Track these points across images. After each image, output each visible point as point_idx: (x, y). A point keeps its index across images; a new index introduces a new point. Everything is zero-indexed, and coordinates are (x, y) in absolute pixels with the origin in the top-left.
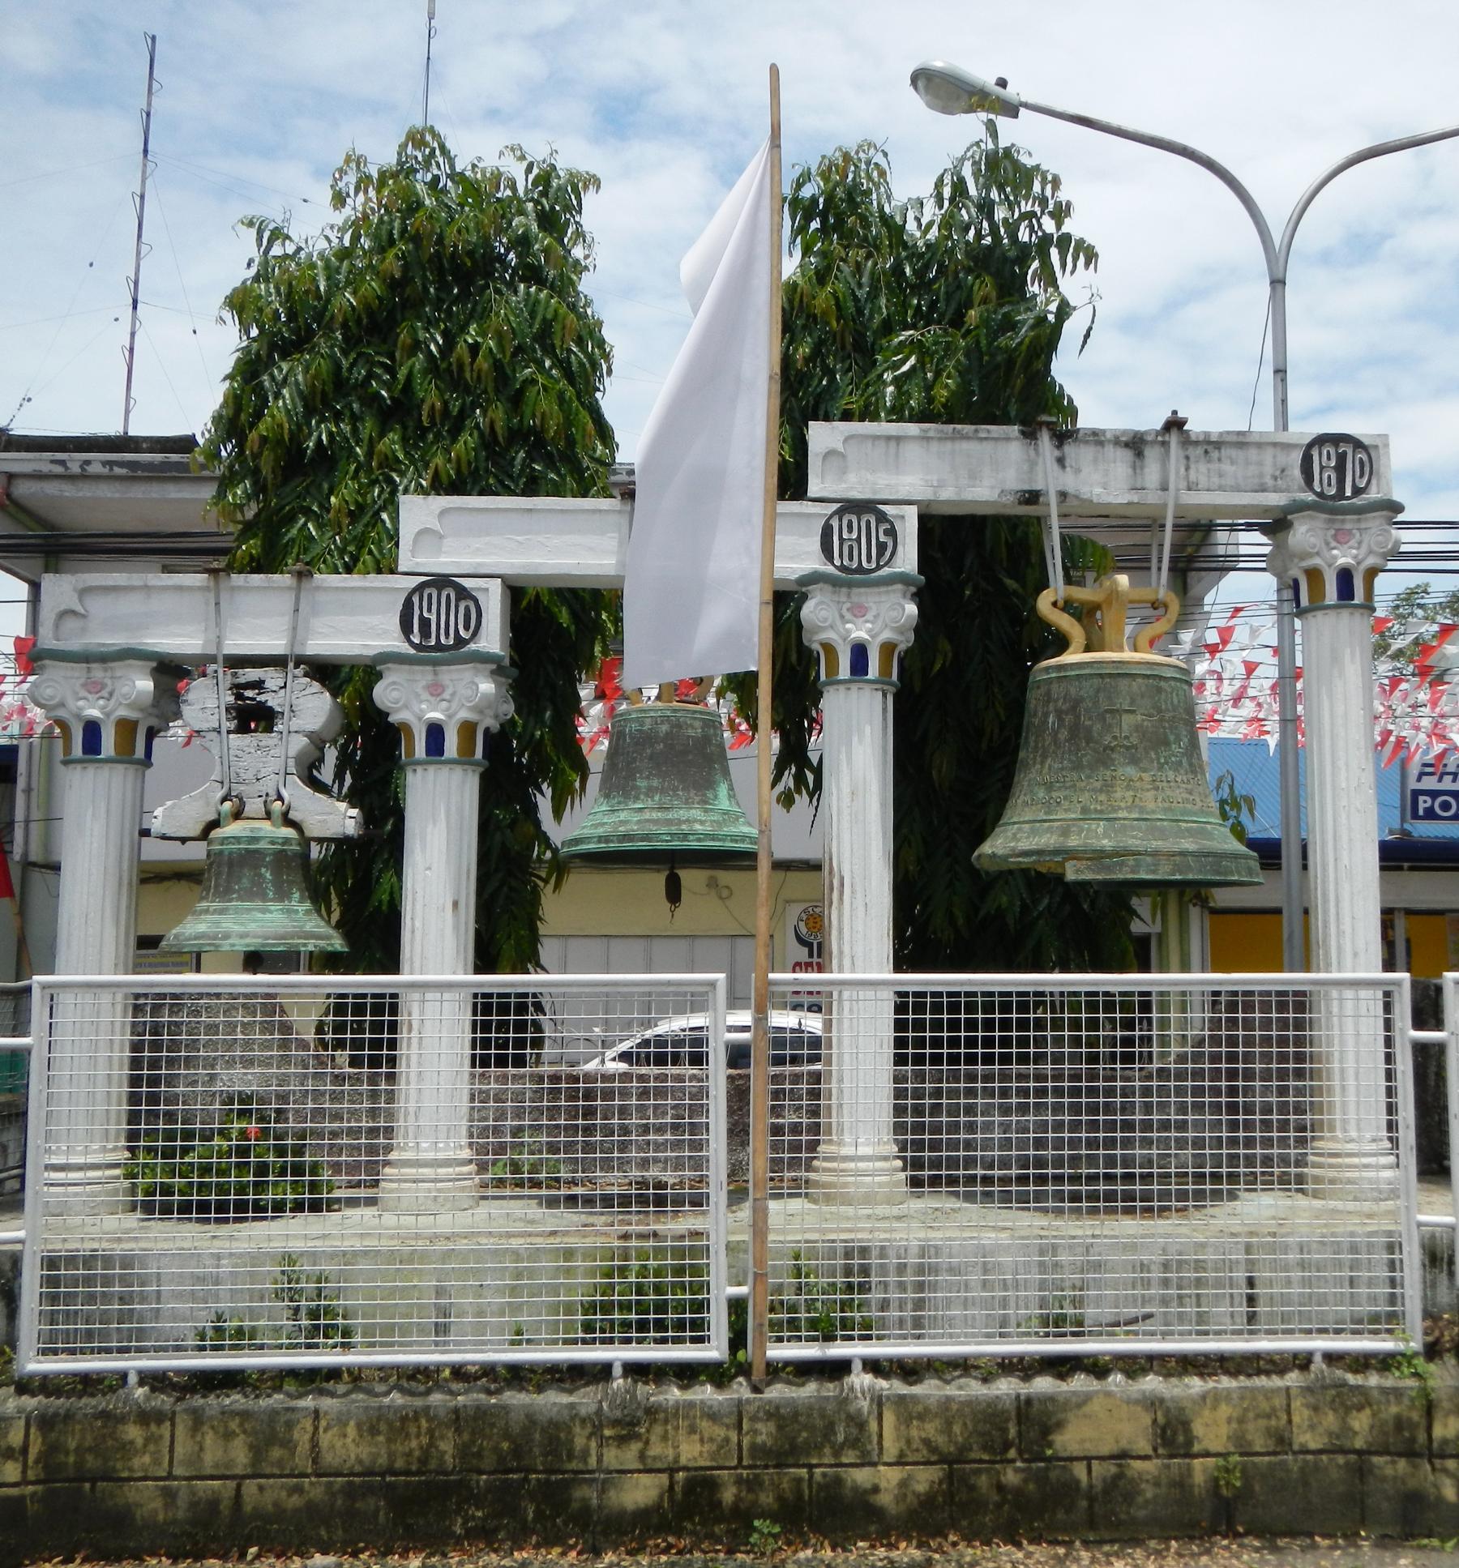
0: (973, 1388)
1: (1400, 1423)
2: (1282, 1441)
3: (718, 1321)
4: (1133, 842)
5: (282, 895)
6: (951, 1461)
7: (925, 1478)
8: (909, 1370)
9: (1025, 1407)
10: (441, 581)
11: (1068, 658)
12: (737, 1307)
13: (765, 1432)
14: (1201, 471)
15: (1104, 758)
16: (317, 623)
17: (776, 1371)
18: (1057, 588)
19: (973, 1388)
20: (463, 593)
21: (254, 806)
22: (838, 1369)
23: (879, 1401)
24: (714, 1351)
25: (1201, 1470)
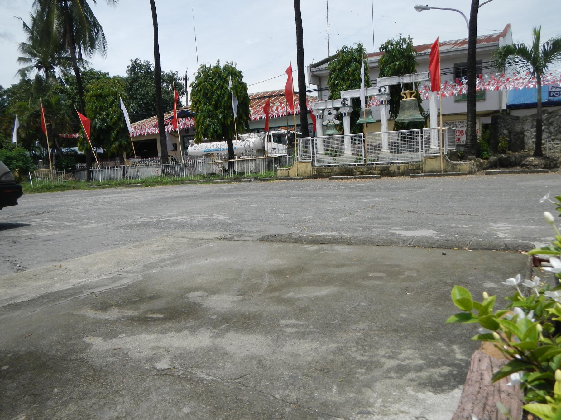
0: (383, 165)
2: (408, 169)
4: (405, 118)
5: (333, 129)
7: (379, 172)
8: (378, 164)
10: (345, 99)
11: (404, 99)
12: (365, 160)
13: (367, 169)
14: (417, 77)
15: (404, 110)
16: (335, 104)
18: (403, 92)
19: (383, 165)
20: (346, 100)
22: (373, 164)
24: (363, 163)
25: (401, 171)
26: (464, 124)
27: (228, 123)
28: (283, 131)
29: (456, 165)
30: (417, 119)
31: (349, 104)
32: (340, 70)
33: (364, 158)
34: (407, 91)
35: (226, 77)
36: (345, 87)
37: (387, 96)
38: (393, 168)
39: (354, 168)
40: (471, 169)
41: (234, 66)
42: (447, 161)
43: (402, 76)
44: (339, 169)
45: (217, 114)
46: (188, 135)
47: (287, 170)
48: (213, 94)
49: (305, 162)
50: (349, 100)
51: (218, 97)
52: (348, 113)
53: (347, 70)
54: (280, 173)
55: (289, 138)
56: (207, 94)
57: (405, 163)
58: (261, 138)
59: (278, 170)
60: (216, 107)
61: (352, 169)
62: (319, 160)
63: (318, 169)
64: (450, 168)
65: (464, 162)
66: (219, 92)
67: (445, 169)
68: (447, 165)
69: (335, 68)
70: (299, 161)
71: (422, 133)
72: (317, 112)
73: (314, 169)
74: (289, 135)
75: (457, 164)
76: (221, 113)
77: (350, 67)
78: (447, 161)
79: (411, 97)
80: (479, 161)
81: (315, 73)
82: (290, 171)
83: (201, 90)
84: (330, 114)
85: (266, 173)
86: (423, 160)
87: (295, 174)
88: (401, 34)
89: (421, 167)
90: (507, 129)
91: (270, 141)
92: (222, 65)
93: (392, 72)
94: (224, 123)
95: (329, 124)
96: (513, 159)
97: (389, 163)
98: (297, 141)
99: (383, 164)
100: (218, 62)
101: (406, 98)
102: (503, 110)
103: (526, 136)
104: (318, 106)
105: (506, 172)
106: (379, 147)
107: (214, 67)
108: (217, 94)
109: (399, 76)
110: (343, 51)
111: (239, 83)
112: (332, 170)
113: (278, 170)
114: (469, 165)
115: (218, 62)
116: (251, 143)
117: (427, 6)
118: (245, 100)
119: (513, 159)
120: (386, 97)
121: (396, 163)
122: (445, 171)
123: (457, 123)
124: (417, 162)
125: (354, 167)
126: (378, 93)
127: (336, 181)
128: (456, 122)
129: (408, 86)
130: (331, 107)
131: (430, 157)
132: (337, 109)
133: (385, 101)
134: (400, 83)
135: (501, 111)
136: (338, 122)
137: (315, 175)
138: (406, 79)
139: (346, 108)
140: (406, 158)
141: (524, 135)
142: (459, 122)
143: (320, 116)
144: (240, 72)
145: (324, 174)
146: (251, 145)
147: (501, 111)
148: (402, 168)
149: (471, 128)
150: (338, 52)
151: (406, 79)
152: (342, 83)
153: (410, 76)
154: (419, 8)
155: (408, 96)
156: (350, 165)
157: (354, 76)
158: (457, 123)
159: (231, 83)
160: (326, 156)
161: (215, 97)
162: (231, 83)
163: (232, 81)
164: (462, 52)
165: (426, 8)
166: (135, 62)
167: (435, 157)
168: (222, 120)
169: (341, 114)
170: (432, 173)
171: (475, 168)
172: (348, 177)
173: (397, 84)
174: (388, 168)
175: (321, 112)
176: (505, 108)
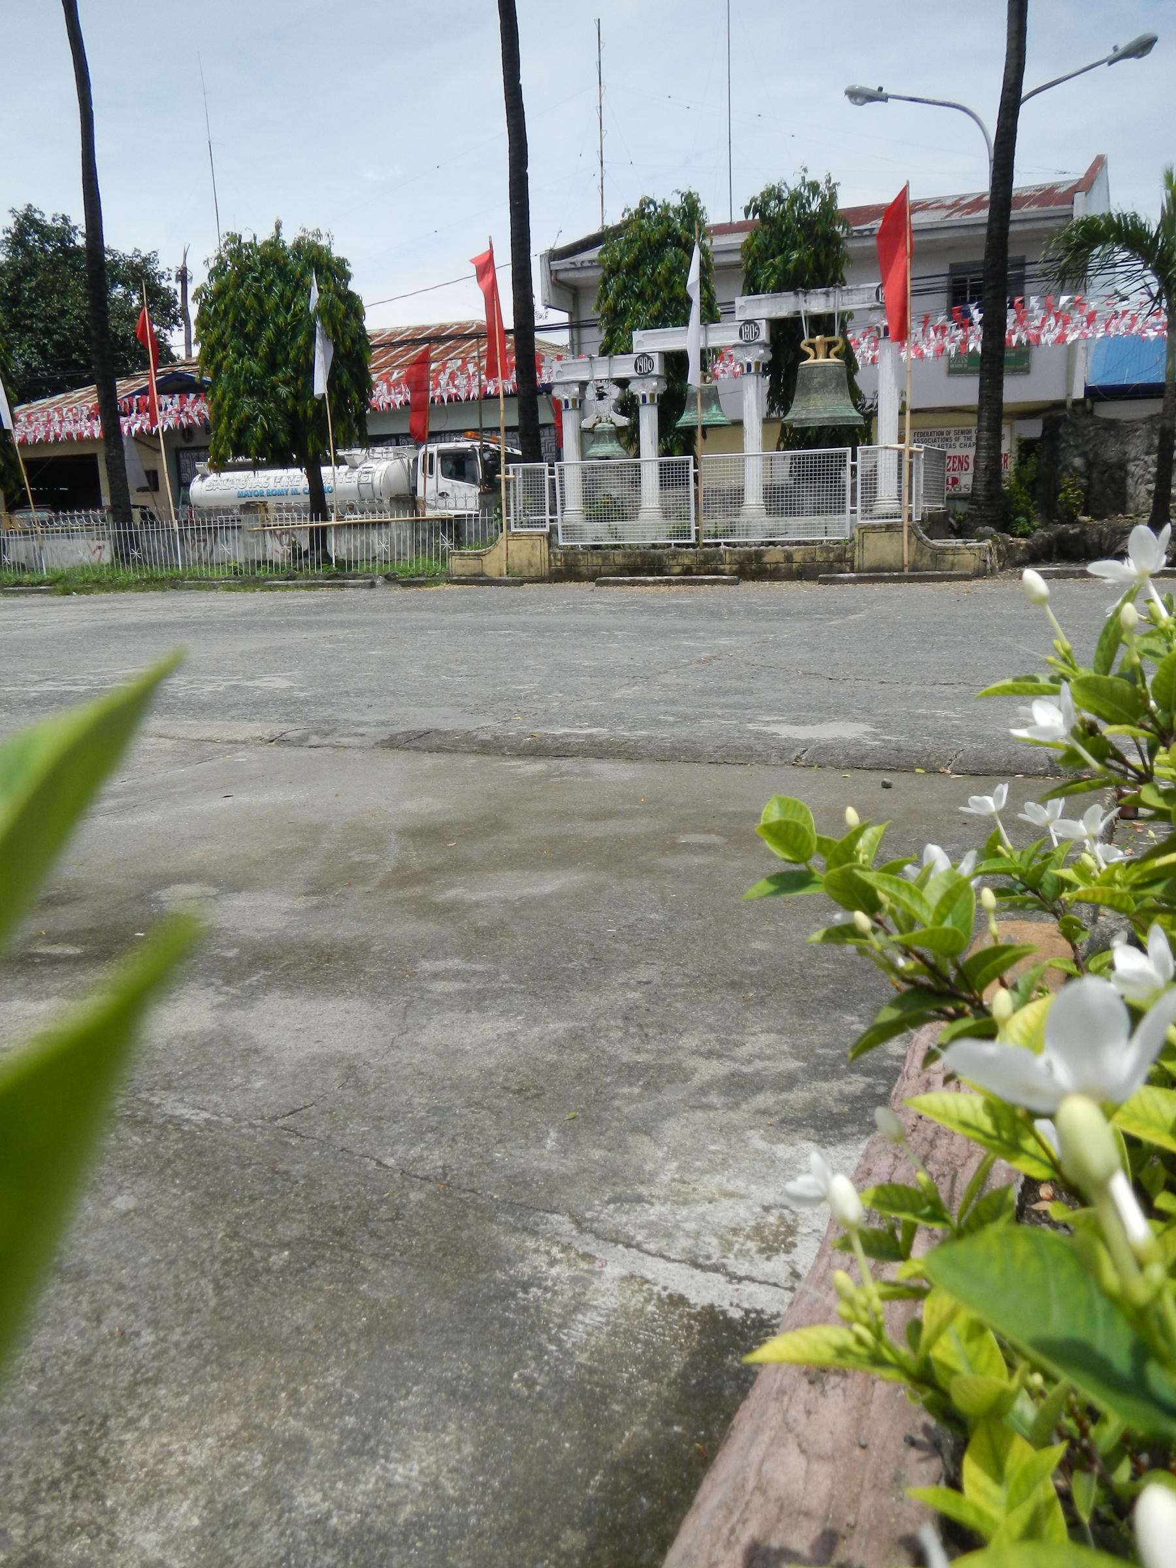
0: (747, 548)
1: (839, 555)
2: (813, 560)
3: (693, 534)
5: (611, 442)
6: (741, 564)
7: (735, 567)
8: (734, 545)
9: (756, 552)
10: (644, 355)
12: (697, 531)
13: (702, 557)
14: (846, 299)
15: (809, 392)
17: (706, 545)
18: (806, 340)
19: (747, 548)
20: (649, 358)
21: (604, 419)
22: (718, 545)
23: (725, 551)
24: (693, 541)
26: (970, 439)
27: (305, 412)
28: (467, 445)
29: (943, 551)
30: (842, 418)
31: (656, 371)
32: (634, 268)
33: (694, 528)
34: (818, 337)
35: (302, 275)
36: (644, 318)
37: (762, 351)
38: (773, 556)
39: (668, 555)
40: (982, 564)
41: (323, 242)
42: (919, 539)
43: (805, 294)
44: (624, 556)
45: (274, 387)
46: (192, 445)
47: (478, 555)
48: (262, 322)
49: (530, 535)
50: (656, 359)
51: (279, 332)
52: (652, 396)
53: (654, 269)
54: (456, 565)
55: (484, 463)
56: (244, 323)
57: (805, 543)
58: (405, 461)
59: (453, 554)
60: (272, 366)
61: (660, 558)
62: (569, 531)
63: (565, 555)
64: (926, 561)
65: (965, 543)
66: (280, 320)
67: (915, 561)
68: (920, 551)
69: (619, 263)
70: (514, 530)
71: (854, 458)
72: (566, 391)
73: (555, 554)
74: (487, 456)
75: (947, 549)
76: (286, 383)
77: (662, 260)
78: (919, 539)
79: (828, 357)
80: (1005, 542)
81: (562, 276)
82: (486, 560)
83: (226, 312)
84: (601, 396)
85: (417, 563)
86: (856, 537)
87: (501, 570)
88: (805, 170)
89: (848, 555)
90: (1083, 455)
91: (431, 472)
92: (289, 238)
93: (778, 282)
94: (295, 412)
95: (599, 425)
96: (1095, 538)
97: (762, 544)
98: (507, 472)
99: (746, 544)
100: (278, 227)
101: (816, 358)
102: (1076, 403)
103: (1133, 475)
104: (568, 374)
105: (1074, 572)
106: (737, 496)
107: (266, 243)
108: (274, 323)
109: (797, 294)
110: (641, 213)
111: (339, 296)
112: (605, 558)
113: (453, 554)
114: (977, 552)
115: (278, 227)
116: (378, 475)
117: (881, 89)
118: (357, 347)
119: (1095, 538)
120: (758, 354)
121: (783, 544)
122: (914, 568)
123: (952, 435)
124: (838, 542)
125: (666, 551)
126: (738, 341)
127: (616, 589)
128: (949, 433)
129: (822, 324)
130: (606, 376)
131: (874, 527)
132: (623, 383)
133: (757, 364)
134: (798, 312)
135: (1069, 405)
136: (623, 421)
137: (559, 572)
138: (817, 304)
139: (647, 381)
140: (810, 529)
141: (1127, 473)
142: (956, 433)
143: (574, 401)
144: (342, 262)
145: (583, 570)
146: (376, 483)
147: (1069, 405)
148: (798, 557)
149: (989, 448)
150: (626, 215)
151: (817, 304)
152: (639, 306)
153: (827, 294)
154: (859, 96)
155: (821, 350)
156: (654, 546)
157: (672, 288)
158: (952, 435)
159: (315, 294)
160: (589, 518)
161: (269, 333)
162: (315, 294)
163: (320, 290)
164: (972, 232)
165: (877, 96)
166: (26, 217)
167: (889, 528)
168: (290, 403)
169: (634, 398)
170: (878, 574)
171: (992, 560)
172: (650, 579)
173: (791, 315)
174: (759, 555)
175: (577, 389)
176: (1082, 396)
